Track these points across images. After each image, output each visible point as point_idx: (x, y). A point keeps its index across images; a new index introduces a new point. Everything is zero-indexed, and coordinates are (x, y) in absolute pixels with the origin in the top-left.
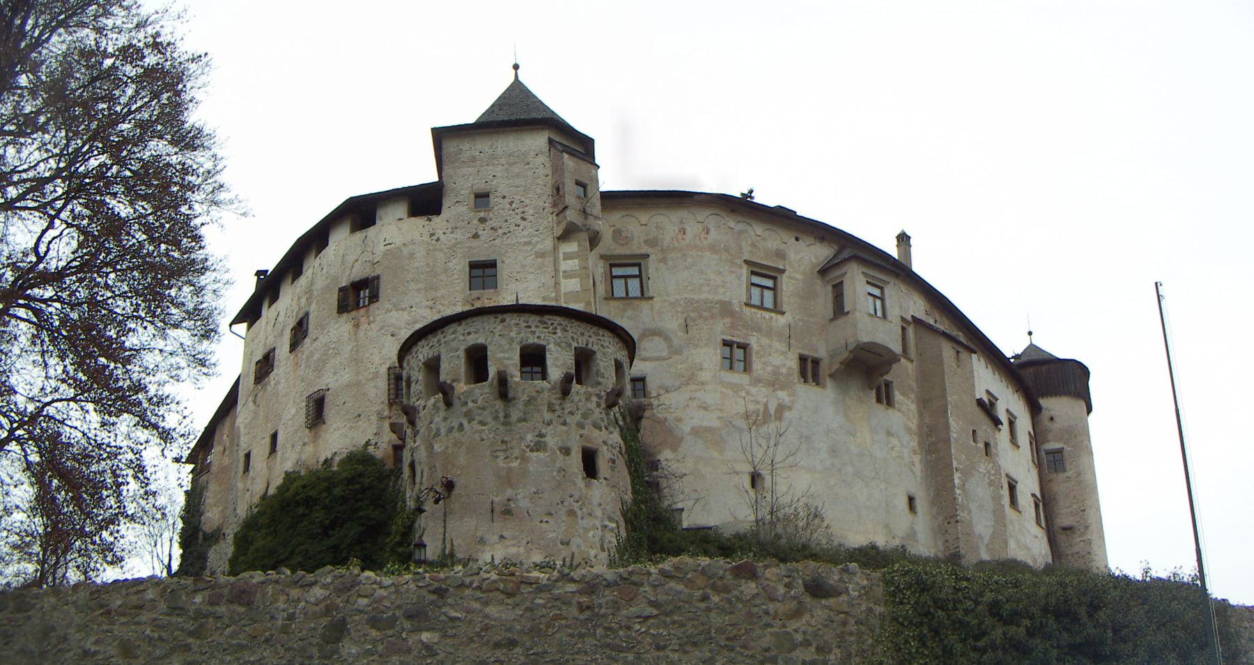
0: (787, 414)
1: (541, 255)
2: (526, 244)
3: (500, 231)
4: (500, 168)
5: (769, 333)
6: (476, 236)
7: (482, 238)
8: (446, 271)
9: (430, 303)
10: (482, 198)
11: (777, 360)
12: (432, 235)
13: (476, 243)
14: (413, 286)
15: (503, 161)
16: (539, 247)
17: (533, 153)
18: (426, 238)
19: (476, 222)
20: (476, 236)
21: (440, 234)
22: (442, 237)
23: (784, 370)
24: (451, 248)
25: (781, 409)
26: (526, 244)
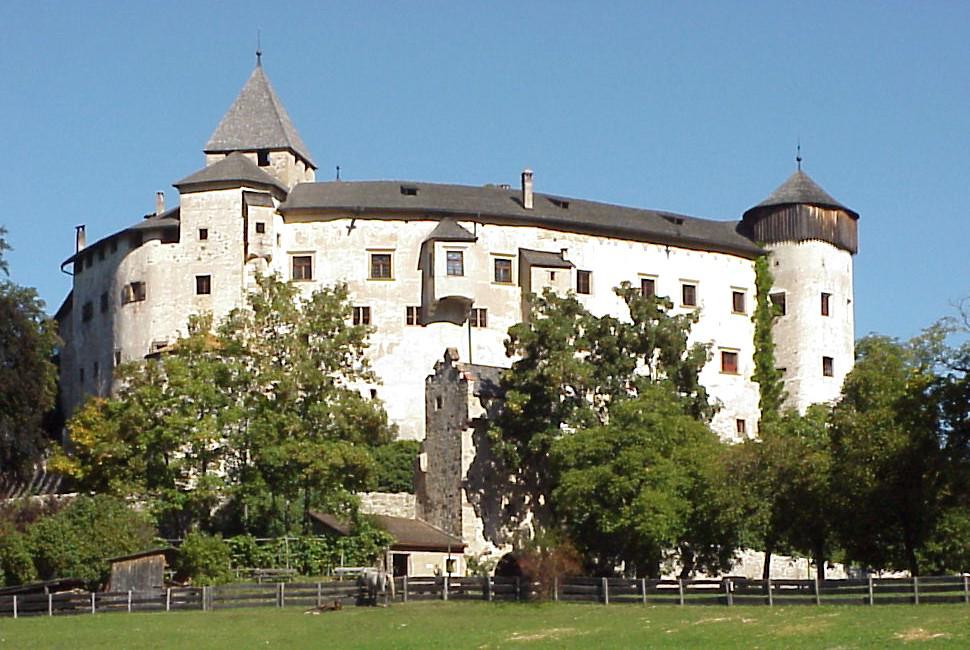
0: (395, 348)
1: (236, 273)
2: (228, 265)
3: (213, 256)
4: (213, 212)
5: (383, 297)
6: (199, 259)
7: (203, 261)
8: (183, 281)
9: (174, 302)
10: (204, 234)
11: (389, 313)
12: (174, 257)
13: (199, 263)
14: (164, 291)
15: (216, 207)
16: (234, 268)
17: (232, 202)
18: (171, 259)
19: (199, 249)
20: (199, 259)
21: (178, 257)
22: (180, 259)
23: (394, 320)
24: (187, 266)
25: (391, 345)
26: (228, 265)
